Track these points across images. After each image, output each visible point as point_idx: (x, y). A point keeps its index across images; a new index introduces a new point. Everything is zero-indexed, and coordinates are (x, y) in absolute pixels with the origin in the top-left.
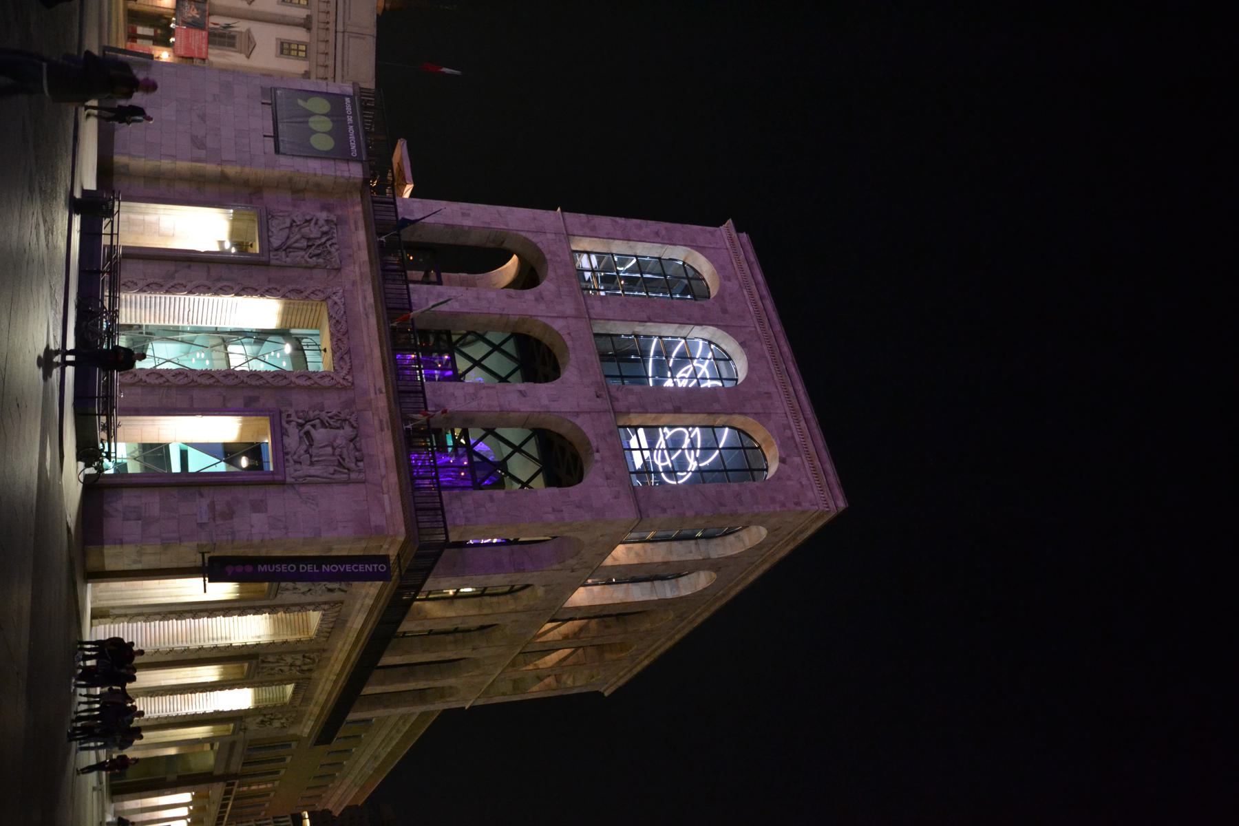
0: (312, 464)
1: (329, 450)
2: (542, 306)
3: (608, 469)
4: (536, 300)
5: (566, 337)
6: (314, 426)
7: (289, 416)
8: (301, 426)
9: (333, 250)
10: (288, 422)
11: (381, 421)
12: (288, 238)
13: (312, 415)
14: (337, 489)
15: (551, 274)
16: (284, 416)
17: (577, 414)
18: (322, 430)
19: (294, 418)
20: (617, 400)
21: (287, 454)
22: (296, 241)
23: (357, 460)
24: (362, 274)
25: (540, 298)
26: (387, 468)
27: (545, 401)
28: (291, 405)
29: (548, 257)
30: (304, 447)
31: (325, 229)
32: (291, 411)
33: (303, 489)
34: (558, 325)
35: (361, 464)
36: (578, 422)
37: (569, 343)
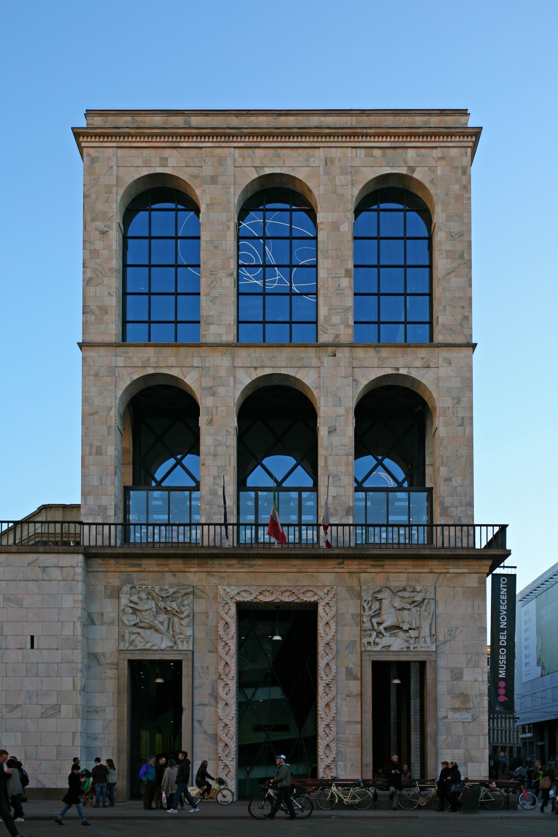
0: (418, 628)
1: (406, 612)
2: (221, 390)
3: (418, 363)
4: (213, 394)
5: (261, 373)
6: (379, 624)
7: (369, 643)
8: (379, 633)
9: (171, 591)
10: (376, 644)
11: (373, 566)
12: (157, 631)
13: (368, 625)
14: (440, 610)
15: (175, 372)
16: (369, 648)
17: (355, 380)
18: (384, 617)
19: (371, 640)
20: (337, 336)
21: (409, 647)
22: (162, 623)
23: (414, 591)
24: (199, 565)
25: (212, 391)
26: (422, 566)
27: (341, 411)
28: (354, 642)
29: (151, 371)
30: (401, 633)
31: (144, 596)
32: (365, 641)
33: (441, 637)
34: (246, 379)
35: (418, 589)
36: (364, 382)
37: (268, 371)
